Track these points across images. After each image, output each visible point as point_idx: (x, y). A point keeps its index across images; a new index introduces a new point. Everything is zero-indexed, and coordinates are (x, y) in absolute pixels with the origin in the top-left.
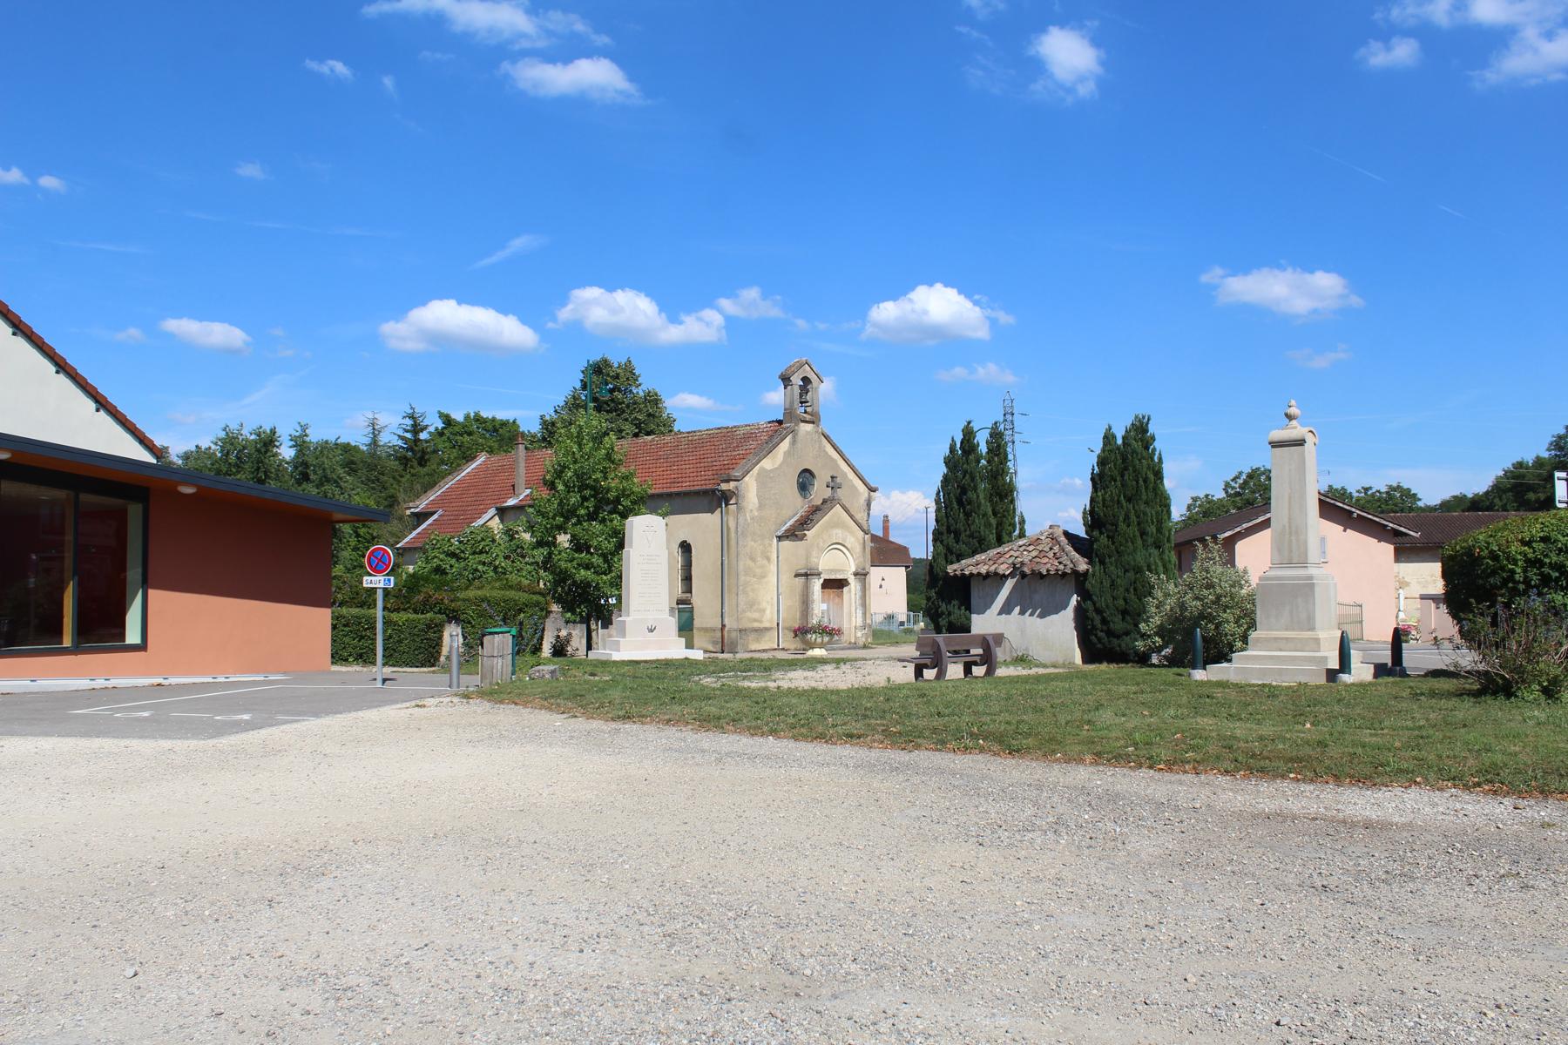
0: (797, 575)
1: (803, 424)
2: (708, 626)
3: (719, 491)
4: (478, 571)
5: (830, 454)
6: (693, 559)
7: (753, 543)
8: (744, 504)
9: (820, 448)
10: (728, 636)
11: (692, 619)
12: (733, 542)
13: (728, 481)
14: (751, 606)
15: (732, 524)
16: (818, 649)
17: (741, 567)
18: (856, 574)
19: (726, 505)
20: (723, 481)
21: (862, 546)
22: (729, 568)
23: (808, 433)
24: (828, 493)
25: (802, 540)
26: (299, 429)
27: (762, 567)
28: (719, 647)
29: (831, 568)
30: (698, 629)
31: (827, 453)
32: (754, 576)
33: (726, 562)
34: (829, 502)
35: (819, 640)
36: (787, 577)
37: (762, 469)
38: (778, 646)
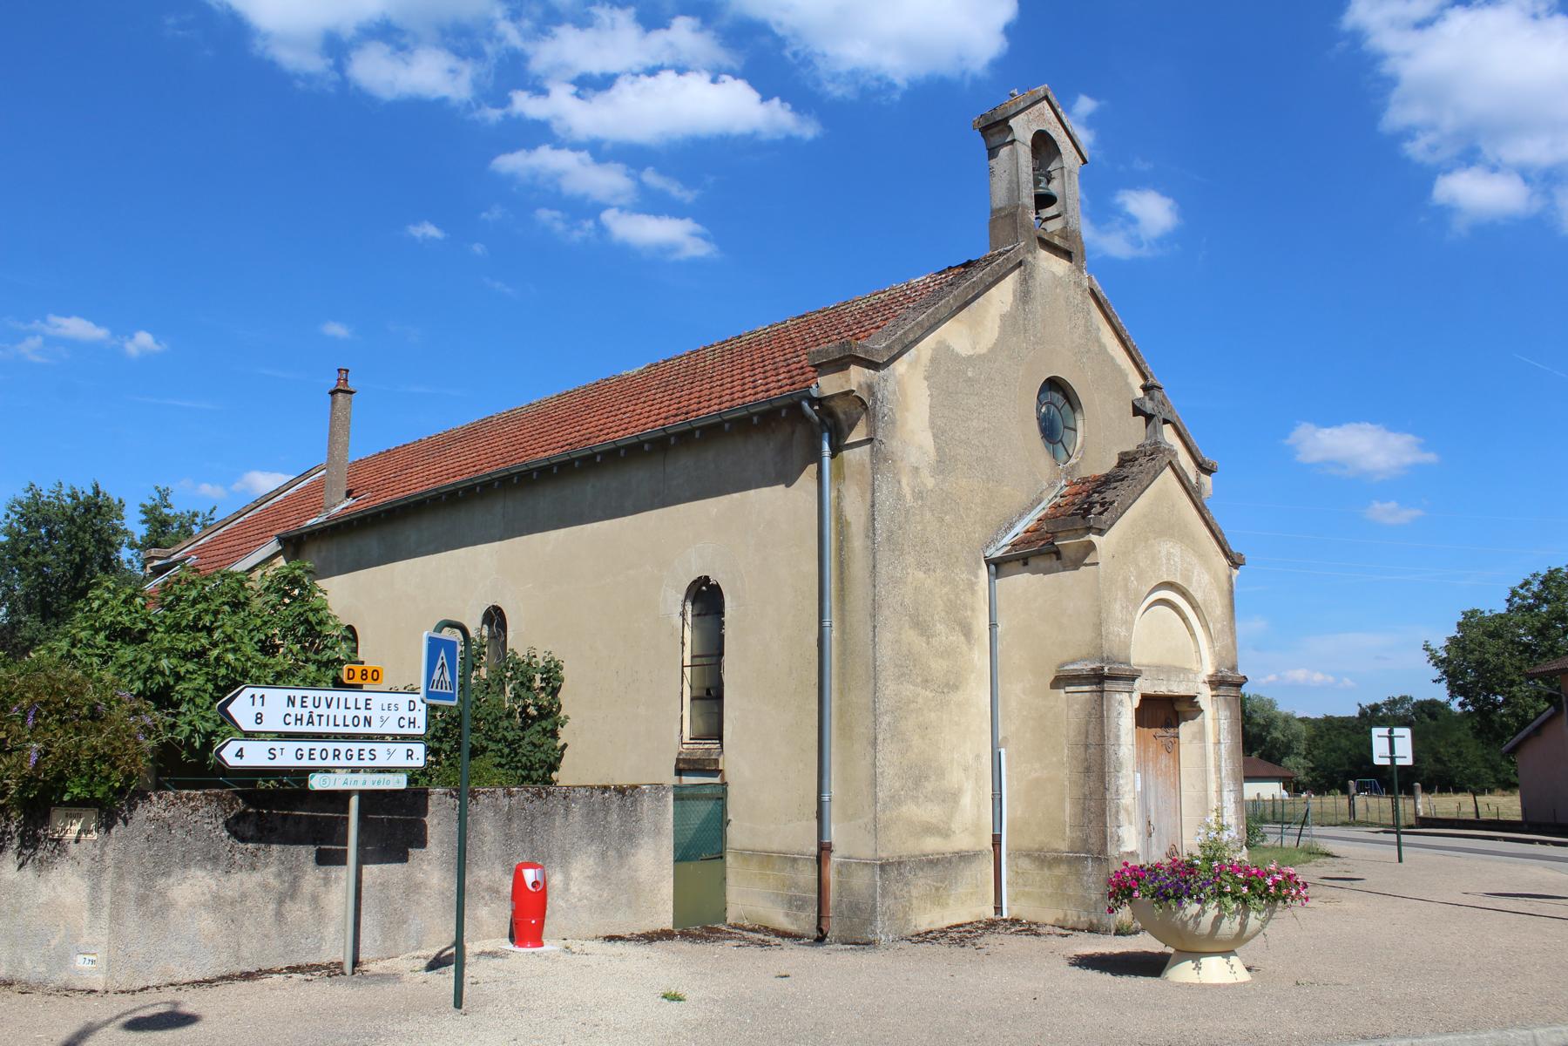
0: (1062, 681)
1: (1043, 254)
2: (775, 847)
3: (813, 401)
4: (162, 674)
6: (729, 632)
7: (921, 575)
8: (894, 445)
10: (840, 884)
11: (719, 822)
12: (858, 567)
13: (840, 364)
14: (919, 781)
15: (855, 509)
16: (1220, 958)
17: (885, 652)
18: (1217, 683)
19: (836, 450)
20: (823, 368)
21: (1226, 601)
22: (843, 653)
23: (1057, 281)
24: (1133, 434)
25: (1077, 564)
26: (156, 496)
27: (948, 653)
28: (805, 922)
30: (748, 855)
33: (833, 635)
34: (1142, 460)
35: (1230, 926)
36: (1024, 690)
37: (944, 351)
38: (998, 909)
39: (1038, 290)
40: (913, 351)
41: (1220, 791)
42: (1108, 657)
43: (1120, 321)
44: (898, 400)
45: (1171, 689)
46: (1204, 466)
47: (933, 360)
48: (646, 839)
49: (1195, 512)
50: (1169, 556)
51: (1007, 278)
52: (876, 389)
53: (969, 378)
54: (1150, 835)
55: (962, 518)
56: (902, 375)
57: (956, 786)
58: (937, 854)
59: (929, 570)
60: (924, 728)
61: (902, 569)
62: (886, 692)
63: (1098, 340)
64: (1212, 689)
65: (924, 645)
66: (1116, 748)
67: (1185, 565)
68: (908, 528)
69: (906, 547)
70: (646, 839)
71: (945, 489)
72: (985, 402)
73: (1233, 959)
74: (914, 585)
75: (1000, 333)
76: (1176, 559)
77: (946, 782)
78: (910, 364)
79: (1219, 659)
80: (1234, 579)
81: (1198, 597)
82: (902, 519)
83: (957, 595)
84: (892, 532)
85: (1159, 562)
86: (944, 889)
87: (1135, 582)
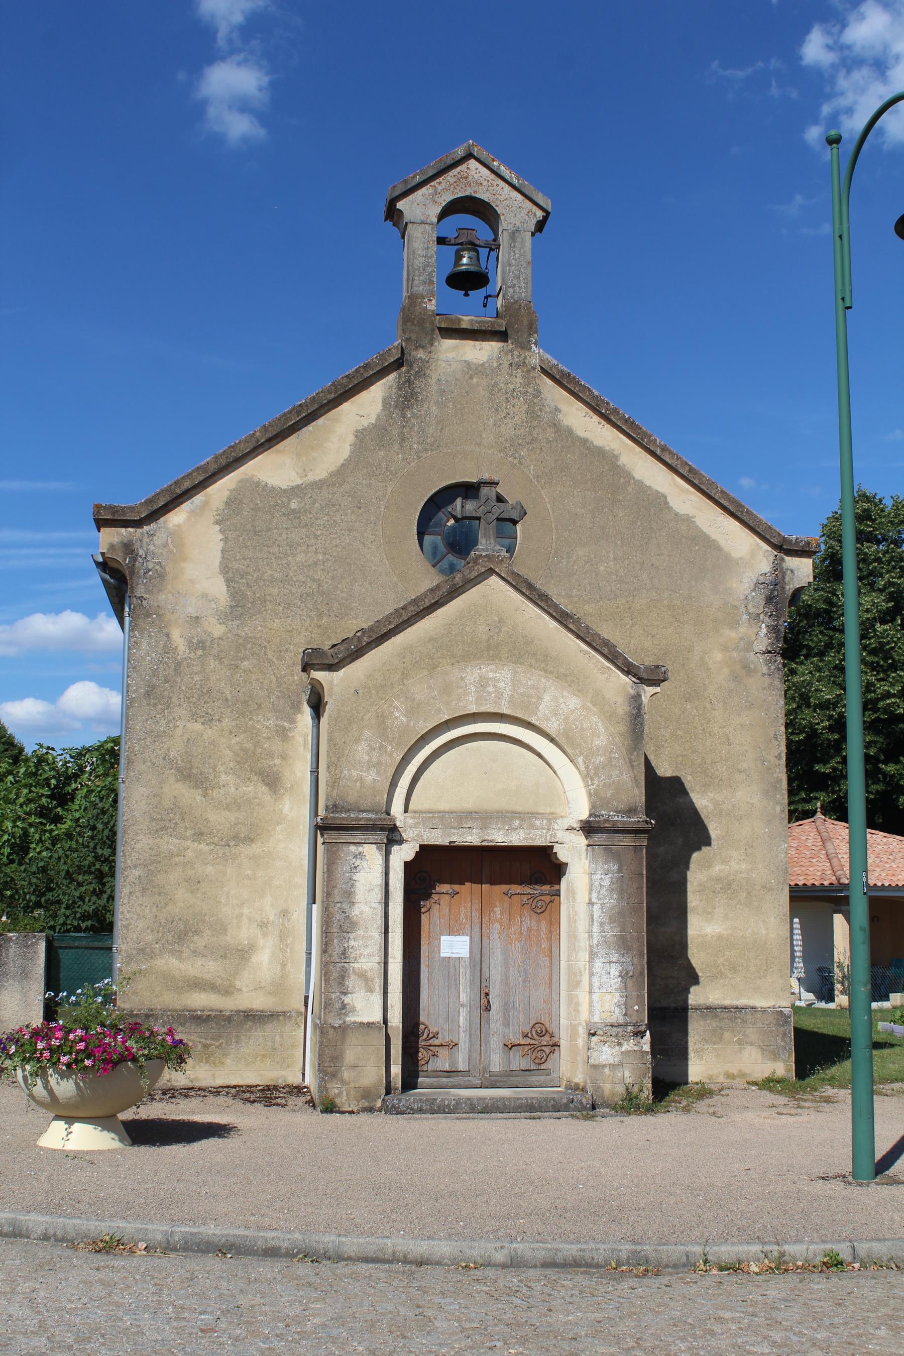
1: (448, 344)
5: (580, 432)
7: (198, 727)
9: (532, 415)
14: (182, 937)
18: (589, 828)
23: (472, 370)
27: (235, 805)
29: (469, 804)
31: (570, 432)
32: (199, 836)
37: (256, 487)
39: (435, 388)
40: (199, 499)
41: (591, 960)
42: (335, 806)
43: (596, 393)
44: (171, 552)
45: (486, 837)
46: (785, 547)
47: (229, 503)
48: (11, 982)
49: (553, 624)
50: (483, 683)
51: (373, 388)
52: (137, 546)
53: (293, 510)
54: (488, 1008)
55: (270, 661)
56: (179, 526)
57: (246, 942)
58: (212, 1010)
59: (211, 720)
60: (194, 883)
61: (168, 723)
62: (137, 846)
63: (556, 426)
64: (587, 838)
65: (199, 798)
66: (345, 906)
67: (522, 690)
68: (179, 680)
69: (175, 700)
70: (11, 982)
71: (243, 634)
72: (319, 533)
73: (77, 1127)
74: (186, 737)
75: (352, 452)
76: (501, 685)
77: (228, 938)
78: (192, 513)
79: (596, 801)
80: (645, 699)
81: (552, 727)
82: (171, 672)
83: (257, 744)
84: (154, 687)
85: (460, 691)
86: (217, 1047)
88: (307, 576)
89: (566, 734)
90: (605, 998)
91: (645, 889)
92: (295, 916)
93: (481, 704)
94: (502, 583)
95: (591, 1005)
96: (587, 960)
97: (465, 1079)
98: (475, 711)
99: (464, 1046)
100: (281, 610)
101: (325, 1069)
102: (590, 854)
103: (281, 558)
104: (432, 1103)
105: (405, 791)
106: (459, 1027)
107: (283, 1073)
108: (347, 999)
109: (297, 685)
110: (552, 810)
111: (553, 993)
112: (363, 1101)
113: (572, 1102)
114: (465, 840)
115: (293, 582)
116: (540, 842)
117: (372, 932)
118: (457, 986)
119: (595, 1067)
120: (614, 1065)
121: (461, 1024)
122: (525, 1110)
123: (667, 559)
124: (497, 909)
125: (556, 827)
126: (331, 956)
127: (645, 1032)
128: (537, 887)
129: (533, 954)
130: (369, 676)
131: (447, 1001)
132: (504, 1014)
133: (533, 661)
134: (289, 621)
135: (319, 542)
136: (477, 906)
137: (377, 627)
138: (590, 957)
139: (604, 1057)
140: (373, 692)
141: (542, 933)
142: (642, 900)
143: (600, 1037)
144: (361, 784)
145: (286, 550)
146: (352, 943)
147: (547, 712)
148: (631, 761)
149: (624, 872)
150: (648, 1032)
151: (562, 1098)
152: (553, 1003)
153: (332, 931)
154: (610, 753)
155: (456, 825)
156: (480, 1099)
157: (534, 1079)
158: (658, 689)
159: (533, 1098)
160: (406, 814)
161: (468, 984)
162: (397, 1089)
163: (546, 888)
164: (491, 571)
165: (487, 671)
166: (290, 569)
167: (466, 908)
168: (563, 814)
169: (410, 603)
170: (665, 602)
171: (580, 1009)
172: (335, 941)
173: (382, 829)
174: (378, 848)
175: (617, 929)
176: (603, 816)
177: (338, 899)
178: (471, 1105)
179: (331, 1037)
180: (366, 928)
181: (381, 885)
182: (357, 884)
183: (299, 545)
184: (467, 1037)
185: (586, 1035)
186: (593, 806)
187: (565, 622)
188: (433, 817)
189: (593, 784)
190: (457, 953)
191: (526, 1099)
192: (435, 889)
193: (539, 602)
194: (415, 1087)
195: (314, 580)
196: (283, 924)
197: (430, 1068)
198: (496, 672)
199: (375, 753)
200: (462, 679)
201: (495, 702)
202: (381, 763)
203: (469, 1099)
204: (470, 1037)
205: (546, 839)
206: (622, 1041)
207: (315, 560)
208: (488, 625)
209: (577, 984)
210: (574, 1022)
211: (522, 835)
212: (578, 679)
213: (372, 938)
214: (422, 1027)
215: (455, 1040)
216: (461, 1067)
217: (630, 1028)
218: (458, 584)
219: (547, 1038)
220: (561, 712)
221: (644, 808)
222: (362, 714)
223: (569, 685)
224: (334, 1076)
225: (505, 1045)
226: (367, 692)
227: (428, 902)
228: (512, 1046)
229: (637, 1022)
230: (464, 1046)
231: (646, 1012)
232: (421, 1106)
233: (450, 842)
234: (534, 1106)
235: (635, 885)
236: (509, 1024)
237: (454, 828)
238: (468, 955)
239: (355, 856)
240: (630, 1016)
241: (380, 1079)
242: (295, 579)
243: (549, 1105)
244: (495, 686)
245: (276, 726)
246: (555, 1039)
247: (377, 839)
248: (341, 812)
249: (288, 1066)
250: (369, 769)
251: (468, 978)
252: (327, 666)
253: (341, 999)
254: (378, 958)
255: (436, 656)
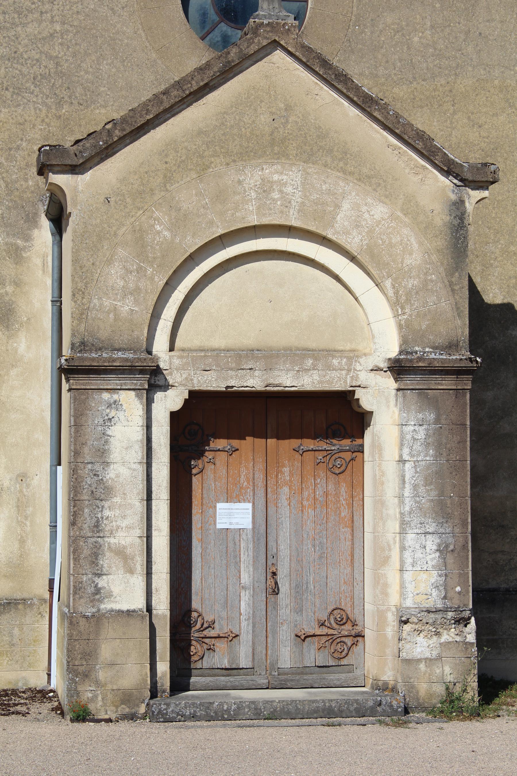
41: (403, 532)
42: (83, 343)
45: (271, 381)
49: (353, 111)
54: (276, 591)
64: (396, 380)
66: (98, 467)
67: (315, 196)
76: (289, 189)
80: (469, 206)
85: (237, 197)
87: (167, 233)
88: (41, 52)
89: (370, 250)
90: (419, 578)
91: (468, 443)
92: (35, 481)
93: (264, 215)
94: (288, 59)
95: (402, 586)
96: (398, 530)
97: (249, 678)
98: (256, 223)
99: (246, 637)
100: (9, 96)
101: (75, 667)
102: (400, 400)
103: (7, 29)
104: (208, 708)
105: (170, 325)
106: (240, 614)
107: (24, 674)
108: (102, 582)
109: (32, 192)
110: (353, 347)
111: (356, 571)
112: (123, 706)
113: (380, 705)
114: (245, 384)
115: (23, 60)
116: (338, 386)
117: (131, 499)
118: (237, 564)
119: (408, 662)
120: (431, 660)
121: (242, 611)
122: (321, 714)
123: (499, 26)
124: (286, 470)
125: (358, 367)
126: (81, 529)
127: (469, 618)
128: (334, 441)
129: (330, 525)
130: (123, 180)
131: (225, 583)
132: (296, 598)
133: (329, 160)
134: (20, 111)
135: (56, 7)
136: (260, 466)
137: (133, 117)
138: (401, 527)
139: (419, 650)
140: (128, 200)
141: (341, 499)
142: (464, 456)
143: (413, 626)
144: (115, 315)
145: (14, 18)
146: (107, 513)
147: (346, 223)
148: (451, 284)
149: (443, 421)
150: (473, 619)
151: (367, 700)
152: (355, 584)
153: (82, 498)
154: (426, 274)
155: (234, 365)
156: (267, 702)
157: (333, 677)
158: (486, 194)
159: (332, 701)
160: (172, 353)
161: (251, 562)
162: (164, 691)
163: (346, 443)
164: (275, 45)
165: (271, 173)
166: (20, 44)
167: (247, 468)
168: (367, 351)
169: (173, 86)
170: (496, 82)
171: (389, 591)
172: (86, 510)
173: (142, 372)
174: (137, 396)
175: (434, 493)
176: (416, 353)
177: (88, 459)
178: (256, 709)
179: (82, 628)
180: (124, 494)
181: (141, 441)
182: (112, 440)
183: (30, 11)
184: (250, 628)
185: (396, 624)
186: (404, 341)
187: (369, 110)
188: (205, 356)
189: (404, 314)
190: (237, 523)
191: (323, 701)
192: (209, 445)
193: (336, 84)
194: (187, 689)
195: (51, 58)
196: (21, 491)
197: (205, 664)
198: (282, 173)
199: (132, 277)
200: (240, 182)
201: (282, 212)
202: (140, 289)
203: (253, 702)
204: (254, 627)
205: (345, 382)
206: (441, 630)
207: (51, 31)
208: (272, 113)
209: (386, 560)
210: (382, 608)
211: (316, 377)
212: (384, 181)
213: (131, 506)
214: (194, 615)
215: (236, 631)
216: (244, 662)
217: (450, 614)
218: (233, 61)
219: (348, 626)
220: (364, 223)
221: (467, 341)
222: (114, 228)
223: (374, 190)
224: (87, 676)
225: (297, 636)
226: (120, 200)
227: (200, 461)
228: (306, 637)
229: (459, 607)
230: (246, 637)
231: (471, 594)
232: (195, 711)
233: (227, 387)
234: (333, 710)
235: (457, 438)
236: (301, 610)
237: (232, 369)
238: (250, 526)
239: (109, 406)
240: (451, 599)
241: (143, 679)
242: (26, 56)
243: (352, 708)
244: (281, 192)
245: (7, 244)
246: (359, 628)
247: (136, 384)
248: (91, 351)
249: (30, 665)
250: (124, 296)
251: (251, 554)
252: (69, 168)
253: (93, 582)
254: (140, 531)
255: (206, 153)
